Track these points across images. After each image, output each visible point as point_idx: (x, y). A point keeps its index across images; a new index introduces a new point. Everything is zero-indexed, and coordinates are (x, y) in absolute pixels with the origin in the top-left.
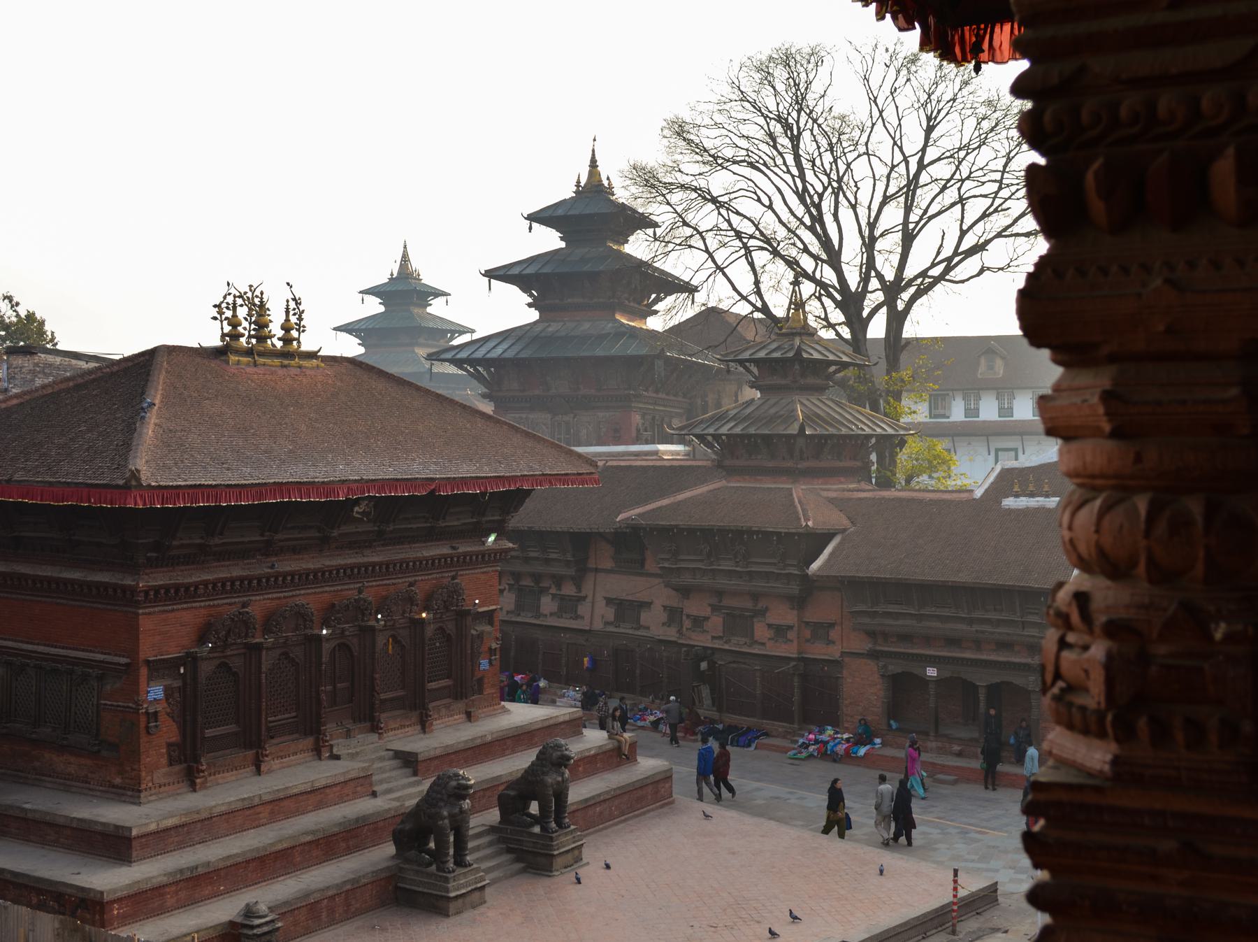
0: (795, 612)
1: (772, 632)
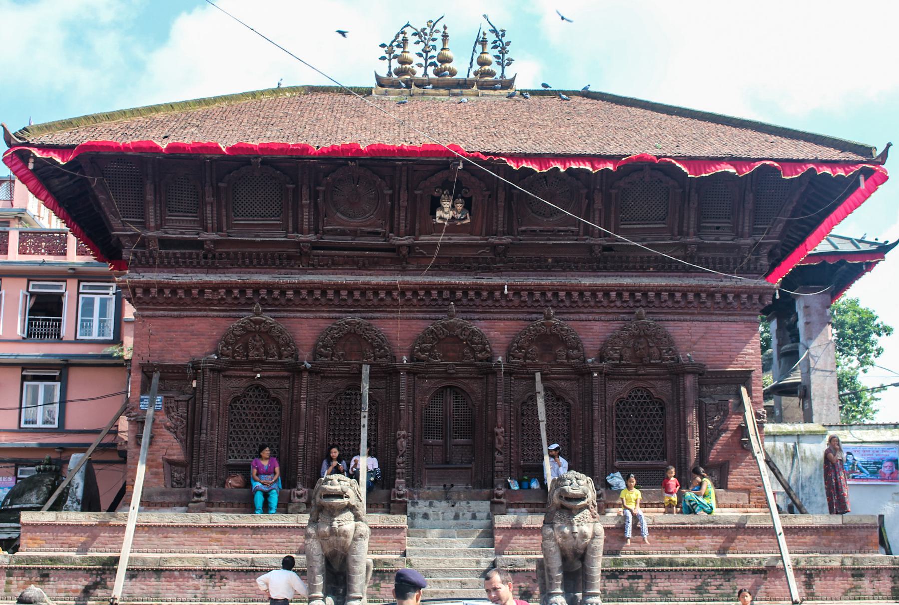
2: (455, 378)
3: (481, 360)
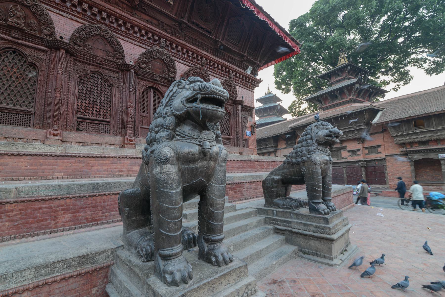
0: (361, 144)
1: (350, 154)
2: (156, 83)
3: (170, 78)
